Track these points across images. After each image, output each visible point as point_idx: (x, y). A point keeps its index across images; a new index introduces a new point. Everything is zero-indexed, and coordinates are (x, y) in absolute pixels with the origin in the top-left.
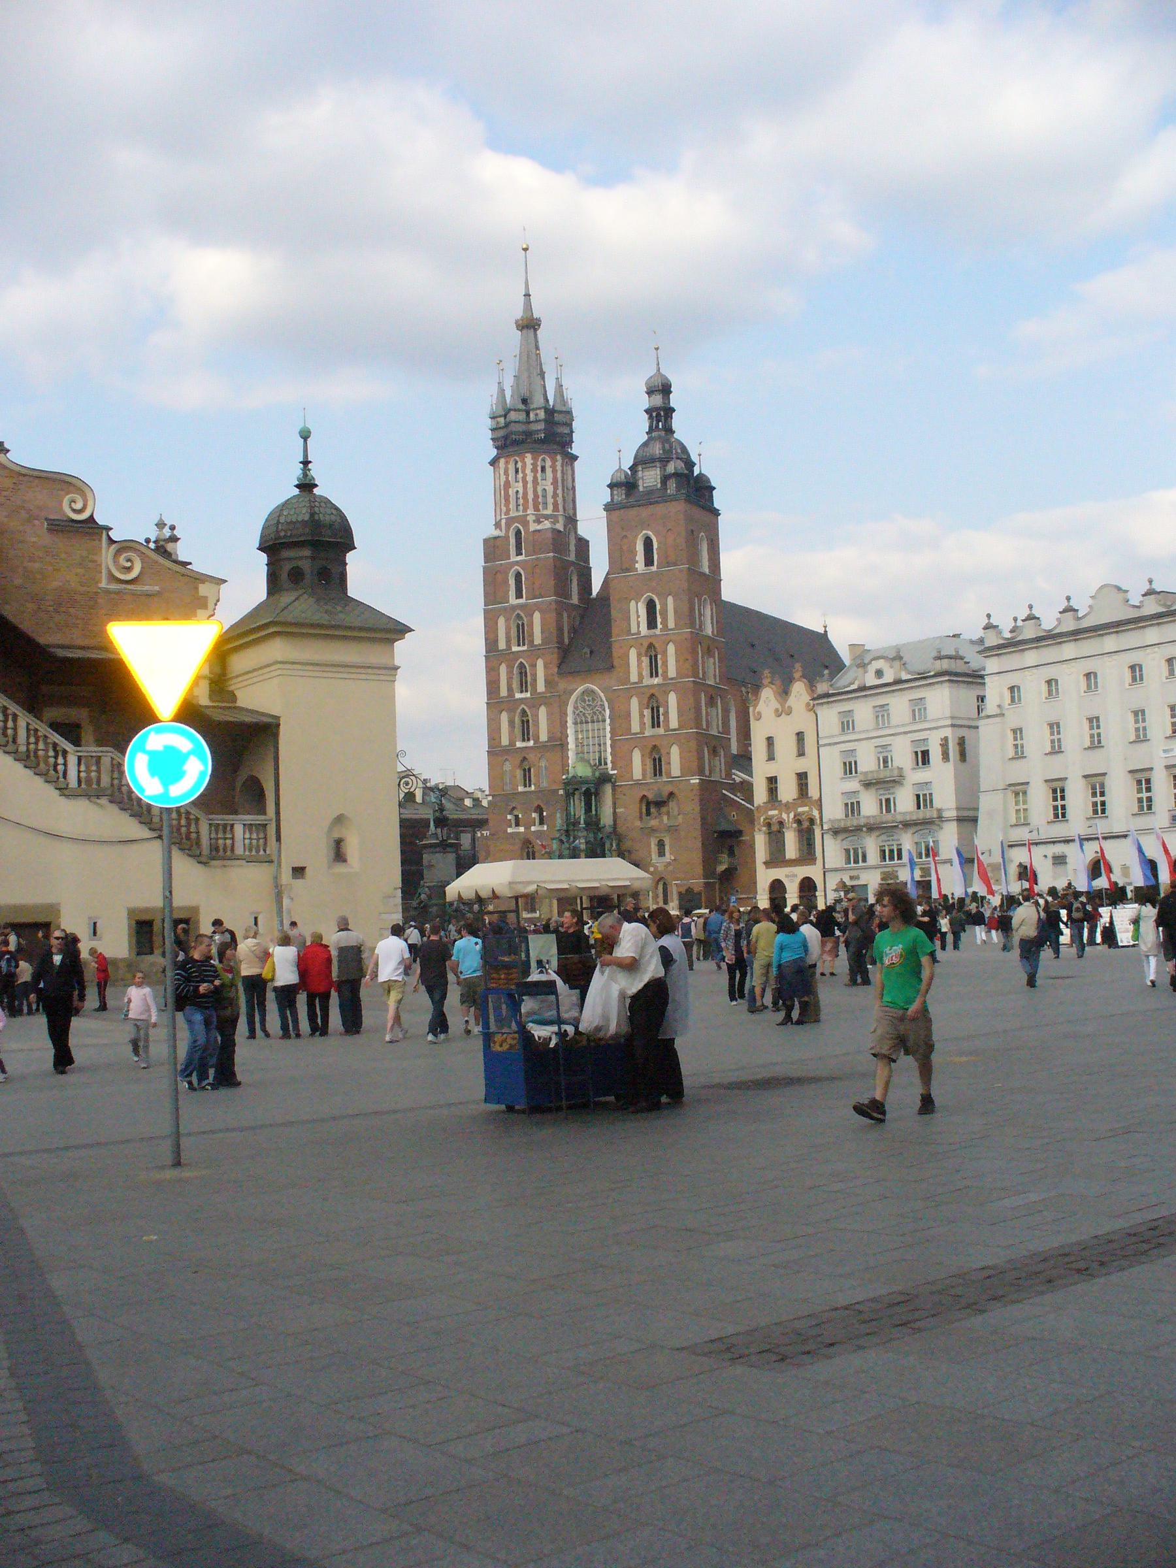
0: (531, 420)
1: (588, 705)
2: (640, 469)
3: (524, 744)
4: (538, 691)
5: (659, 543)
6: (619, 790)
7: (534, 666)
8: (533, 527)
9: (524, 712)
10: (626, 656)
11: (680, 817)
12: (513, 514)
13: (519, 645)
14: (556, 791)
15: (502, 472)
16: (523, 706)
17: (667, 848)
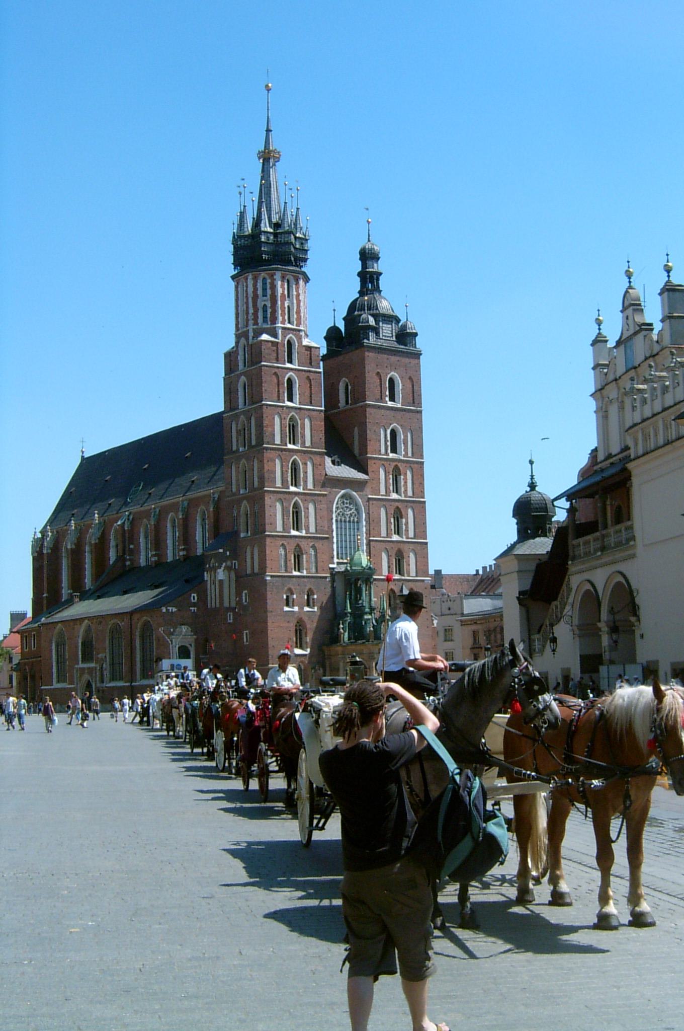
1: (346, 507)
4: (309, 488)
7: (306, 464)
9: (296, 505)
10: (379, 471)
13: (290, 443)
14: (326, 578)
16: (296, 498)
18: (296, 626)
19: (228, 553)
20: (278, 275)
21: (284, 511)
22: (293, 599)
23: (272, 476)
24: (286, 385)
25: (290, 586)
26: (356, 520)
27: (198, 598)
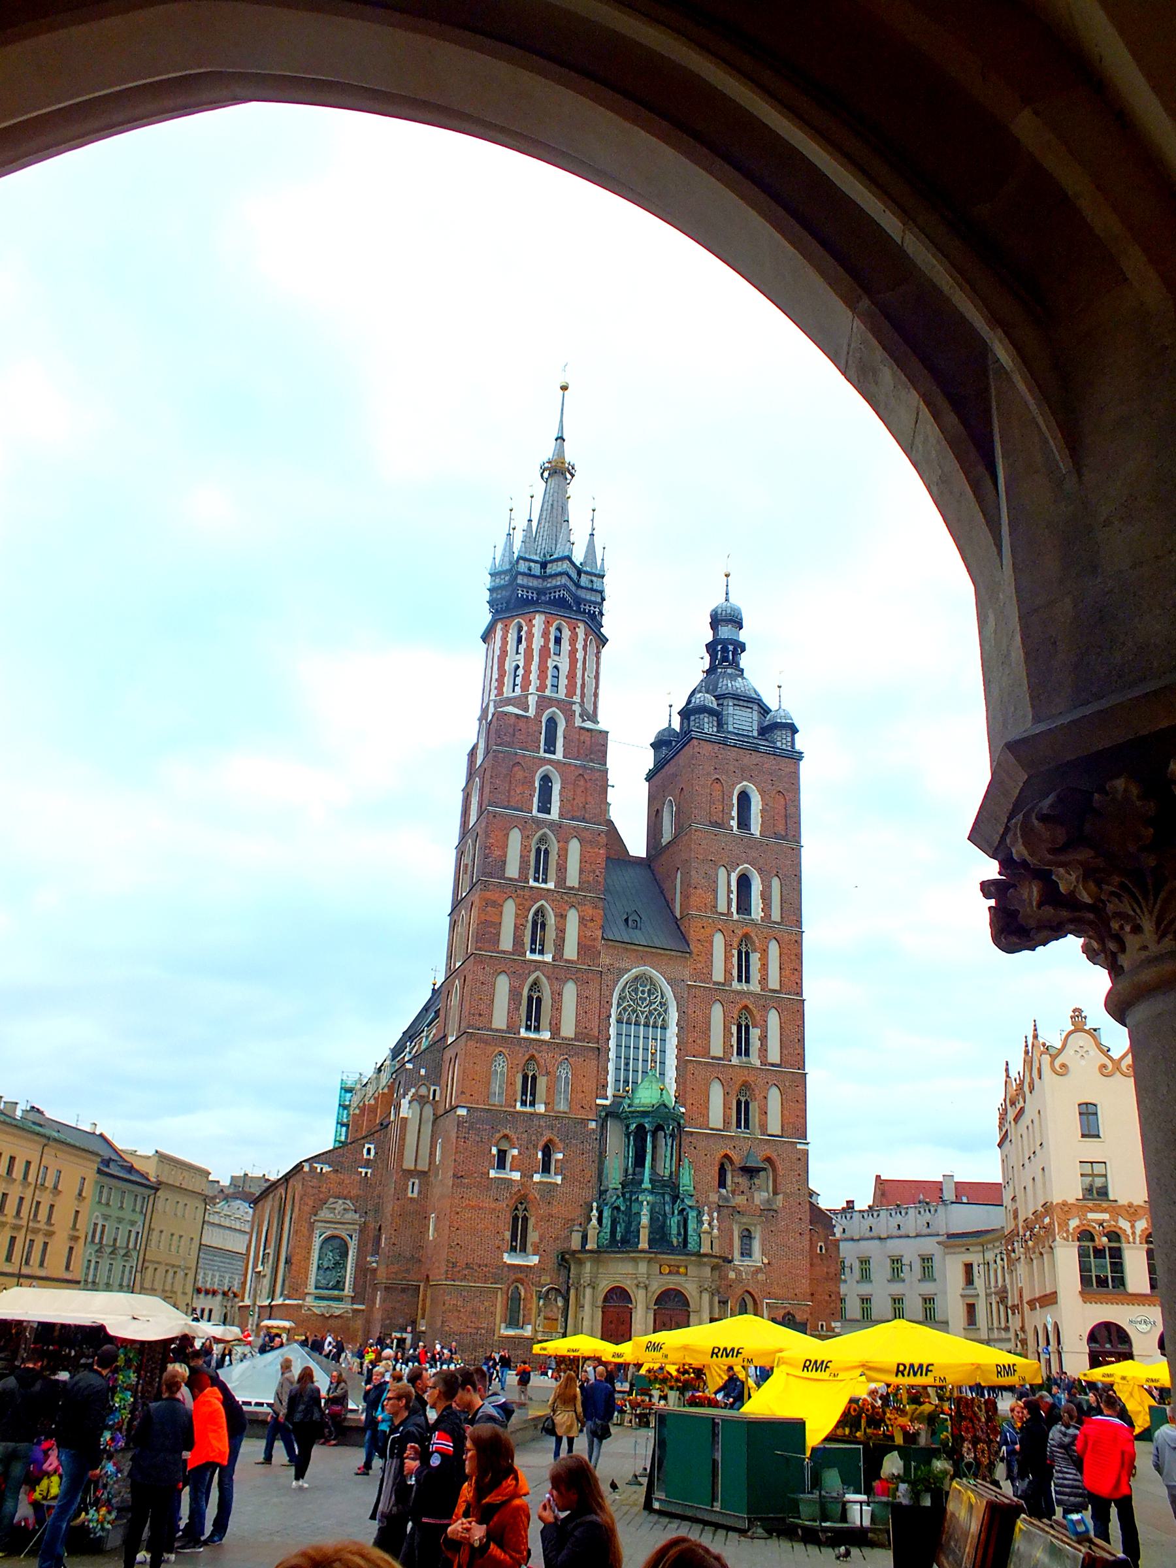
0: (582, 584)
2: (731, 704)
3: (532, 1035)
4: (565, 957)
5: (765, 804)
6: (686, 1140)
7: (562, 917)
8: (578, 722)
9: (535, 984)
11: (780, 1197)
12: (548, 693)
13: (536, 880)
14: (584, 1122)
15: (537, 631)
16: (538, 973)
17: (756, 1246)
18: (516, 1209)
19: (423, 1072)
20: (539, 620)
21: (514, 994)
22: (513, 1156)
23: (492, 930)
24: (537, 785)
25: (507, 1131)
26: (660, 1023)
27: (376, 1153)
